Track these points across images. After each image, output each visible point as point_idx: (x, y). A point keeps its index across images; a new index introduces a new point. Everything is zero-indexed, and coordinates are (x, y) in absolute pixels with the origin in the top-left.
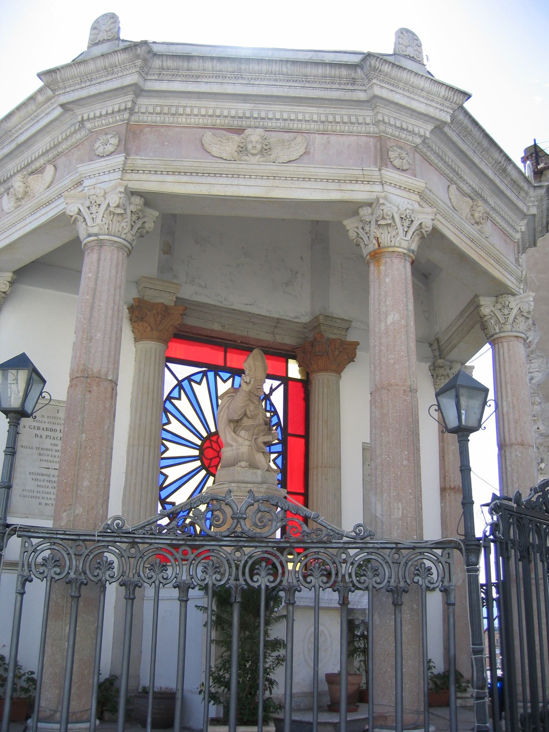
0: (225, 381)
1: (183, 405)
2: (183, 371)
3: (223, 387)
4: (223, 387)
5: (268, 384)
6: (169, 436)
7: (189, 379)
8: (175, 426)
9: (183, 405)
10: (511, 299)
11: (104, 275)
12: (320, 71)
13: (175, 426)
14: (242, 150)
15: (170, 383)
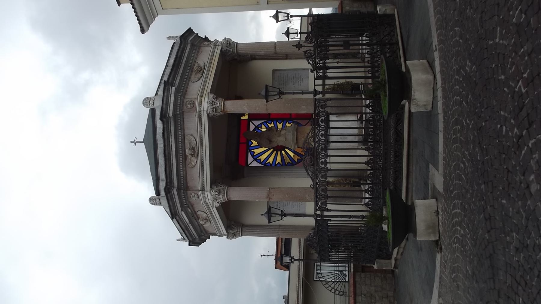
0: (252, 143)
1: (263, 157)
2: (250, 159)
3: (255, 143)
4: (255, 143)
5: (252, 127)
6: (274, 163)
7: (253, 156)
8: (271, 160)
9: (263, 157)
10: (223, 49)
11: (237, 194)
12: (166, 133)
13: (271, 160)
14: (193, 155)
15: (255, 164)
